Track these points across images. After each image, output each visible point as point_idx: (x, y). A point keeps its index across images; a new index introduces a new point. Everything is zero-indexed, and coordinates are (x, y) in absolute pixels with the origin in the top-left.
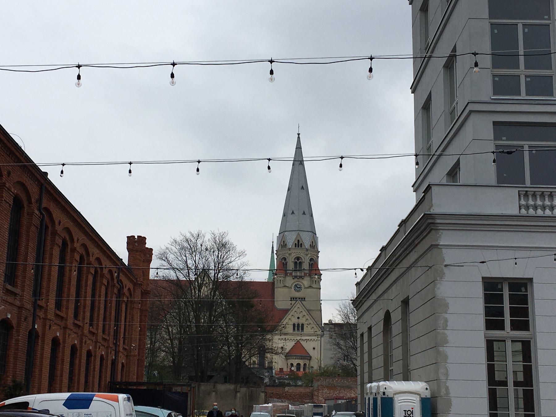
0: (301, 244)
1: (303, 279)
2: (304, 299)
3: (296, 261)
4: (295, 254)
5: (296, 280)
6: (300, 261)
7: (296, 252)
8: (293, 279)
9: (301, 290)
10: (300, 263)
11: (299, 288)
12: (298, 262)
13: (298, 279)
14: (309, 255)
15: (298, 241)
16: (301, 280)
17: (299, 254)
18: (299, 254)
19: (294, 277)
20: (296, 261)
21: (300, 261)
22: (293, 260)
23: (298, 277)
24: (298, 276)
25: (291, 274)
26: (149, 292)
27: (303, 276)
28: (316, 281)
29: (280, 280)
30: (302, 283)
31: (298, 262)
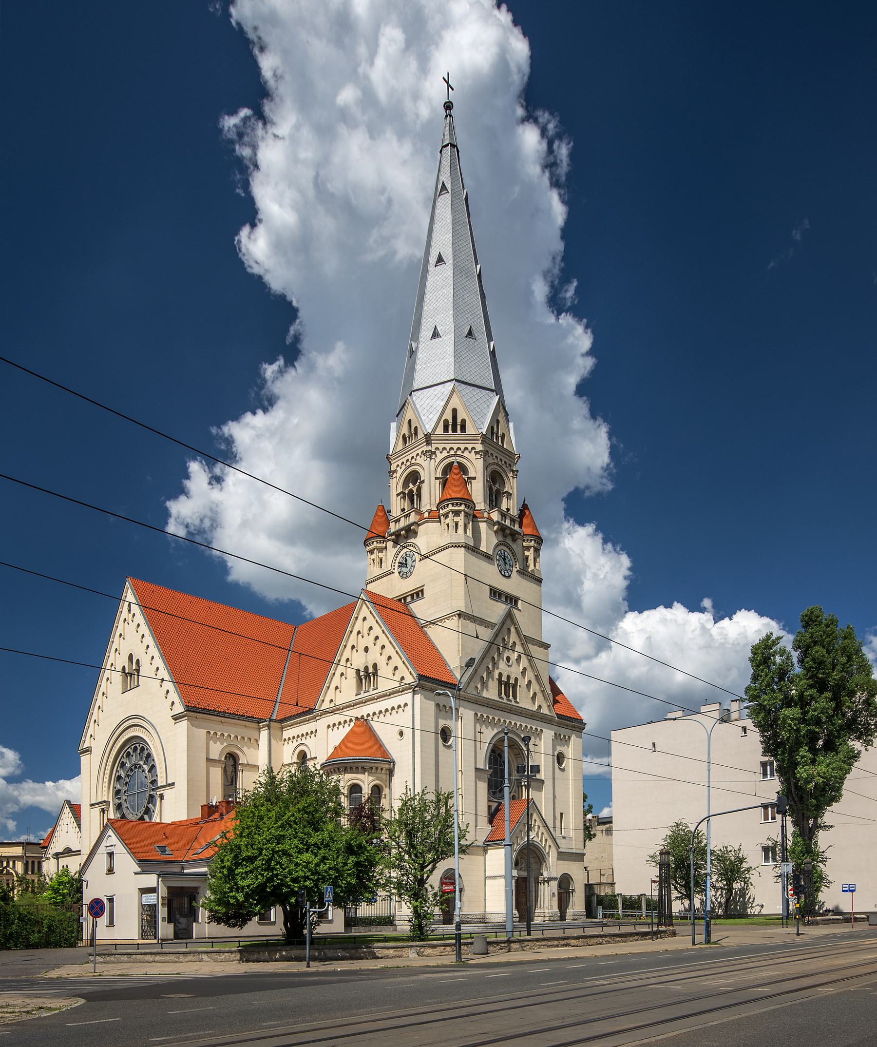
0: (416, 428)
2: (422, 591)
4: (404, 467)
9: (414, 567)
10: (419, 489)
12: (415, 490)
14: (440, 456)
19: (393, 537)
20: (411, 486)
24: (402, 530)
26: (504, 679)
30: (414, 545)
31: (415, 490)
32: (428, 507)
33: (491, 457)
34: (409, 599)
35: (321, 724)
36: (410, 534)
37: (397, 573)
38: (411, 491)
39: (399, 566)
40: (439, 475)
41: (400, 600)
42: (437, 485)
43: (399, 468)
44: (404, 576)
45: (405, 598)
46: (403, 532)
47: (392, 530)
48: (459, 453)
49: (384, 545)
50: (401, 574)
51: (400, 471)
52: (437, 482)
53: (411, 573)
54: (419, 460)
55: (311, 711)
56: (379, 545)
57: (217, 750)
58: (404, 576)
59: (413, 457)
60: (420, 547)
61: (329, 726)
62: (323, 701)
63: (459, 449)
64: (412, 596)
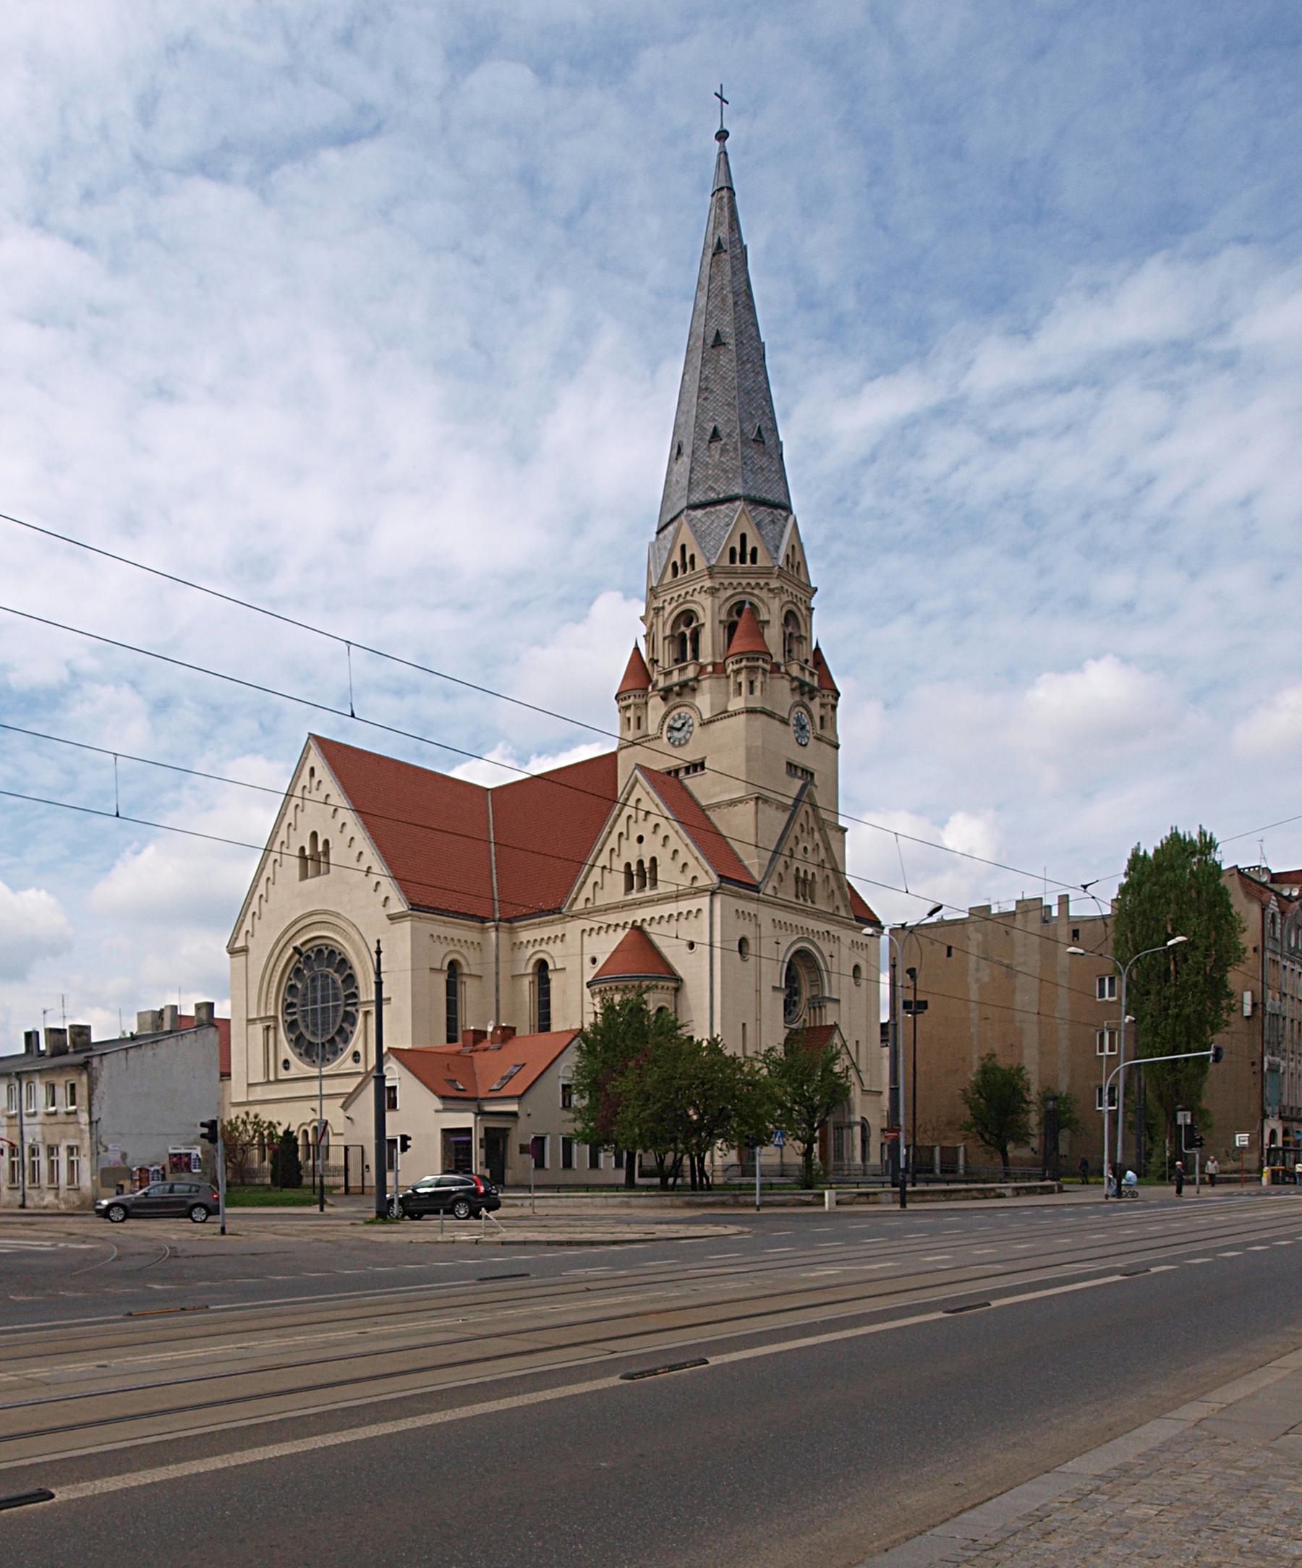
4: (674, 604)
5: (675, 700)
6: (694, 625)
7: (675, 595)
8: (664, 699)
11: (683, 725)
12: (688, 633)
13: (679, 695)
16: (687, 699)
19: (662, 693)
20: (683, 628)
22: (668, 632)
23: (676, 689)
24: (676, 685)
30: (692, 706)
31: (688, 633)
32: (709, 660)
33: (786, 595)
34: (682, 774)
35: (573, 928)
36: (686, 690)
37: (665, 739)
38: (683, 635)
39: (668, 731)
40: (723, 617)
41: (669, 773)
42: (722, 631)
43: (666, 604)
44: (677, 743)
45: (677, 771)
46: (676, 689)
47: (661, 685)
48: (748, 590)
49: (644, 701)
50: (672, 741)
51: (668, 609)
52: (722, 626)
53: (687, 741)
54: (697, 597)
55: (557, 910)
56: (638, 701)
57: (440, 955)
58: (677, 743)
59: (687, 593)
60: (702, 711)
61: (584, 931)
62: (576, 899)
63: (749, 584)
64: (687, 770)
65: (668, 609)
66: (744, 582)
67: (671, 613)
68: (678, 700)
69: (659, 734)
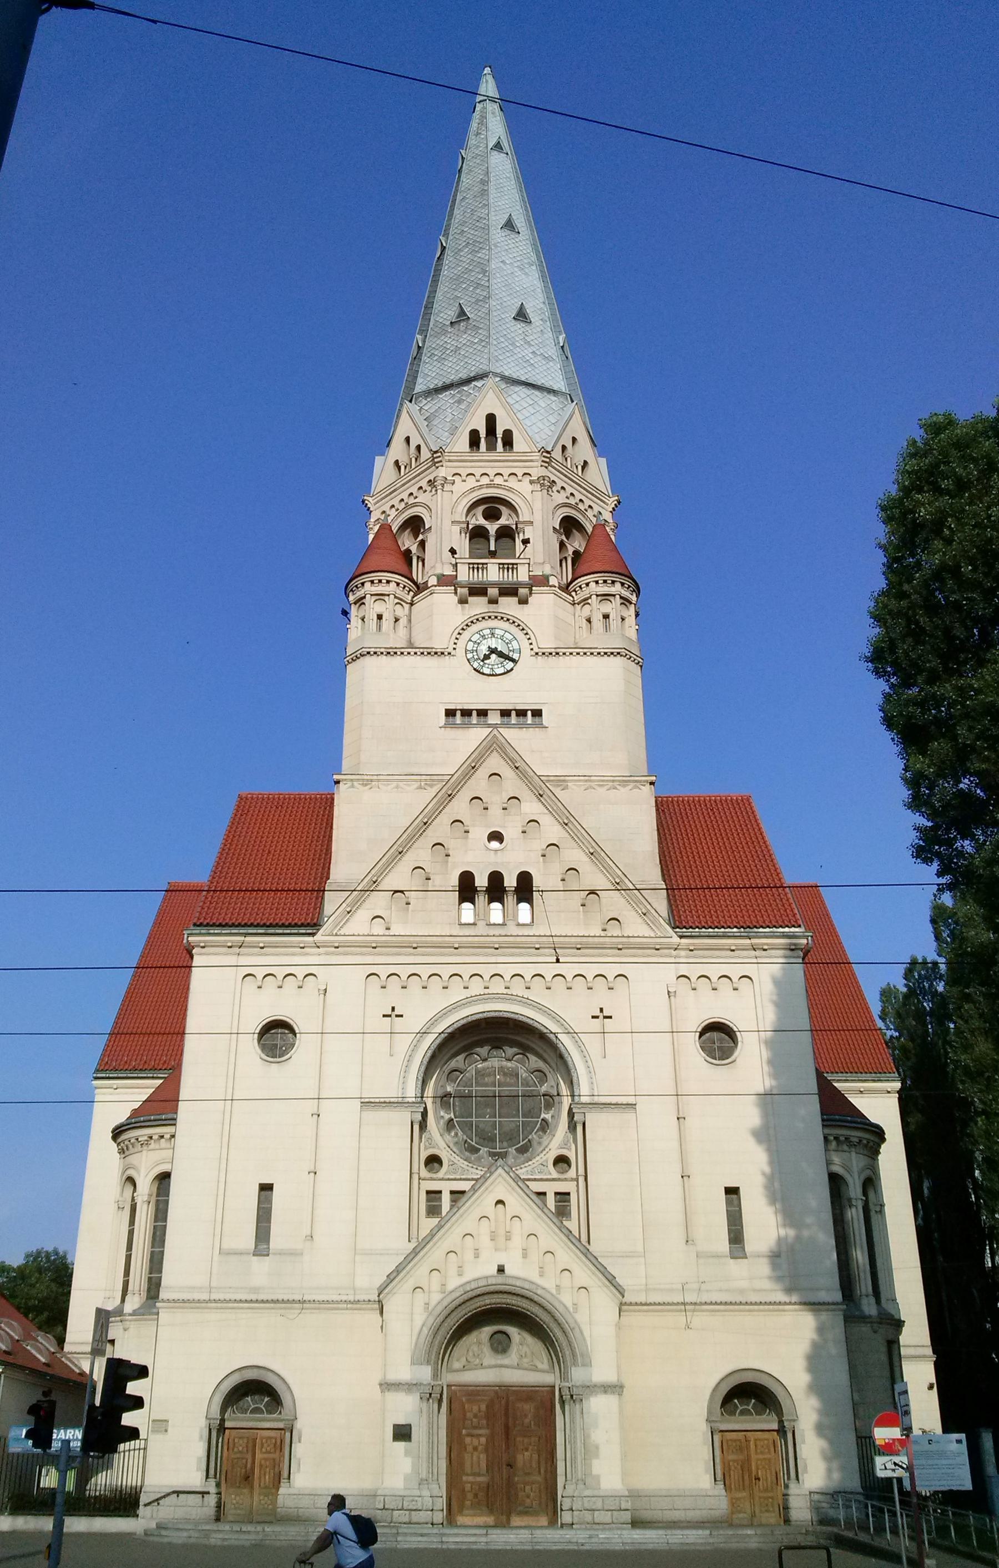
1: (524, 601)
2: (537, 713)
3: (482, 521)
4: (471, 483)
5: (478, 605)
6: (503, 521)
7: (478, 472)
8: (463, 601)
13: (493, 601)
15: (491, 420)
17: (498, 480)
18: (498, 480)
20: (482, 521)
21: (503, 521)
22: (460, 515)
24: (493, 585)
25: (444, 581)
27: (522, 585)
28: (606, 617)
29: (380, 617)
31: (492, 528)
43: (457, 478)
46: (493, 592)
64: (505, 713)
65: (460, 487)
66: (578, 496)
67: (464, 494)
68: (493, 607)
69: (450, 650)
